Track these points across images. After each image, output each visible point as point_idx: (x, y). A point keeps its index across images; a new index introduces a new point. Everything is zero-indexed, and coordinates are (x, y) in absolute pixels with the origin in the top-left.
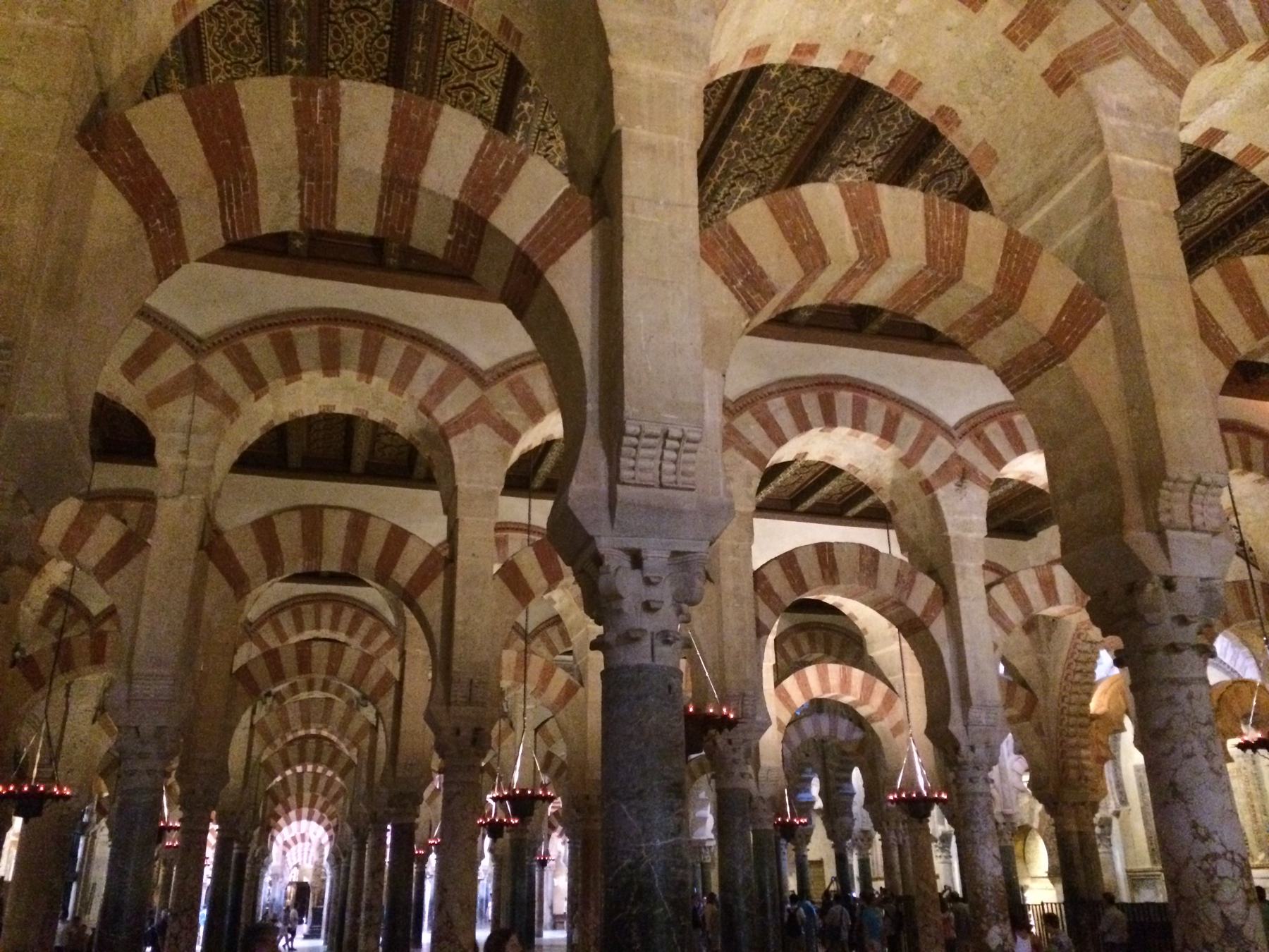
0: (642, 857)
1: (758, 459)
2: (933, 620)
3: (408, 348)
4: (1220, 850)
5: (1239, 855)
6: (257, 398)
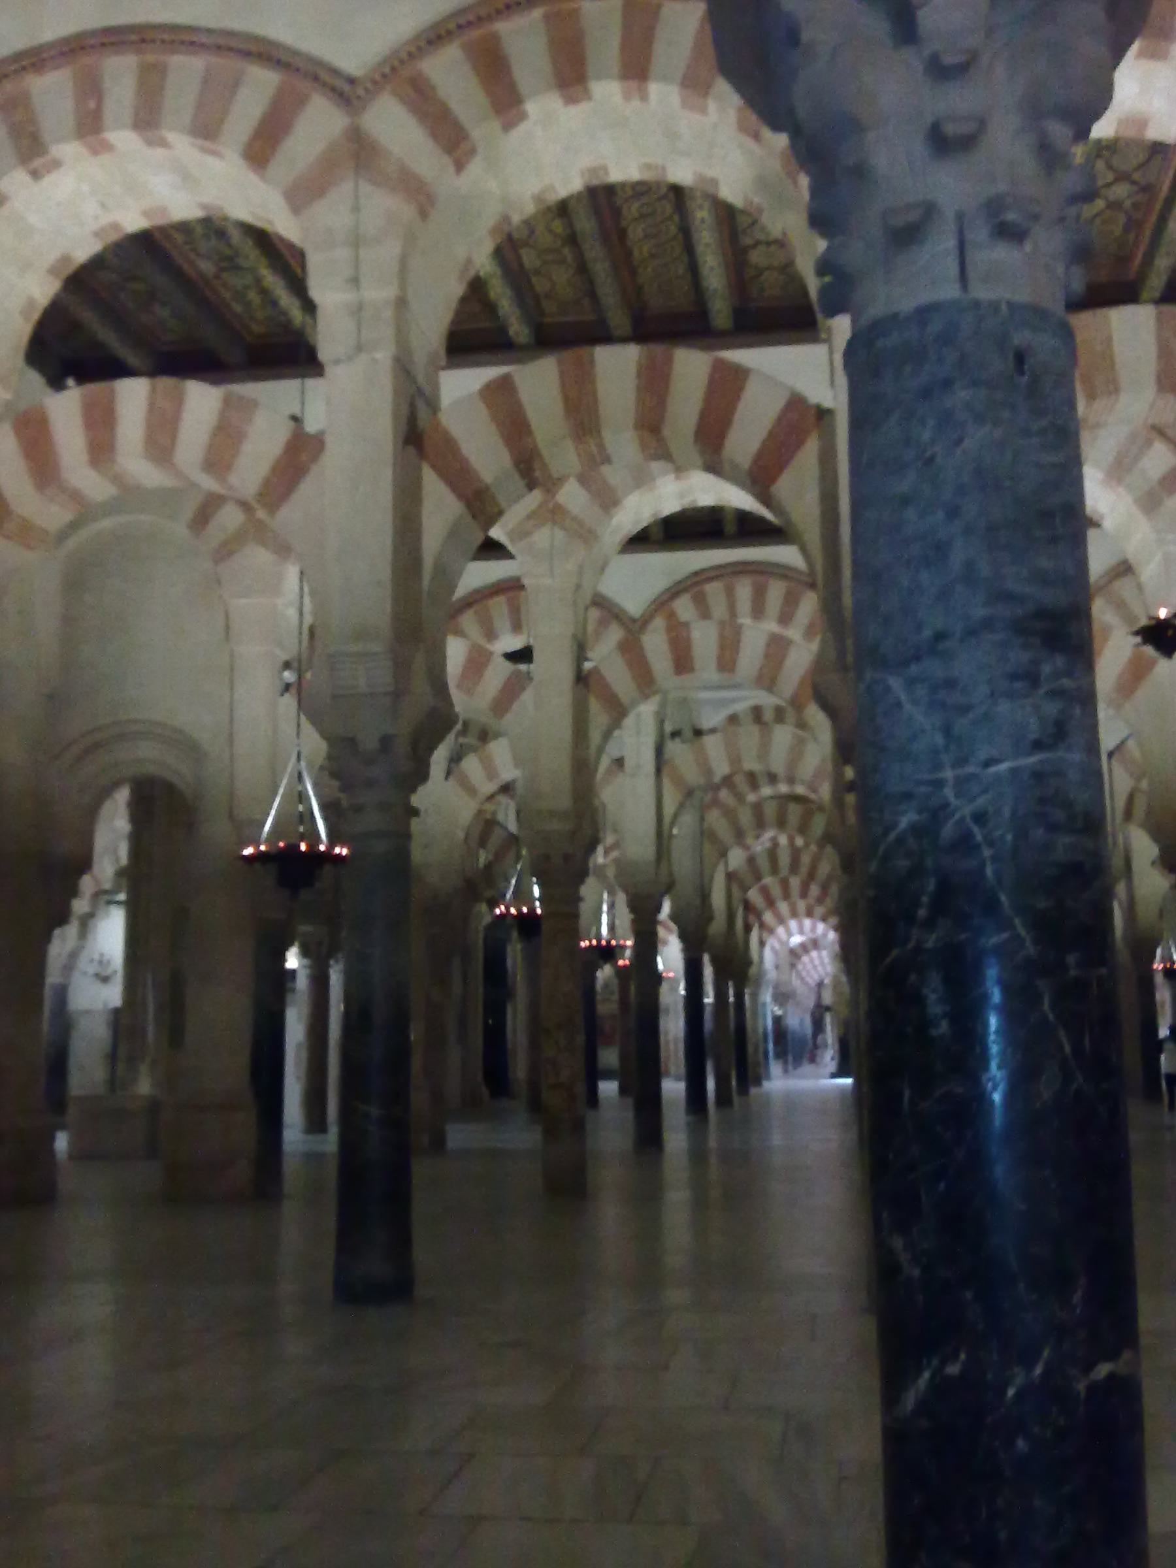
0: (946, 805)
6: (460, 167)
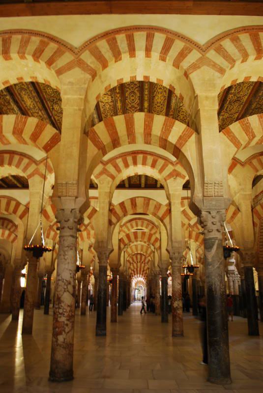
1: (113, 178)
2: (165, 218)
3: (20, 158)
4: (61, 278)
5: (66, 280)
